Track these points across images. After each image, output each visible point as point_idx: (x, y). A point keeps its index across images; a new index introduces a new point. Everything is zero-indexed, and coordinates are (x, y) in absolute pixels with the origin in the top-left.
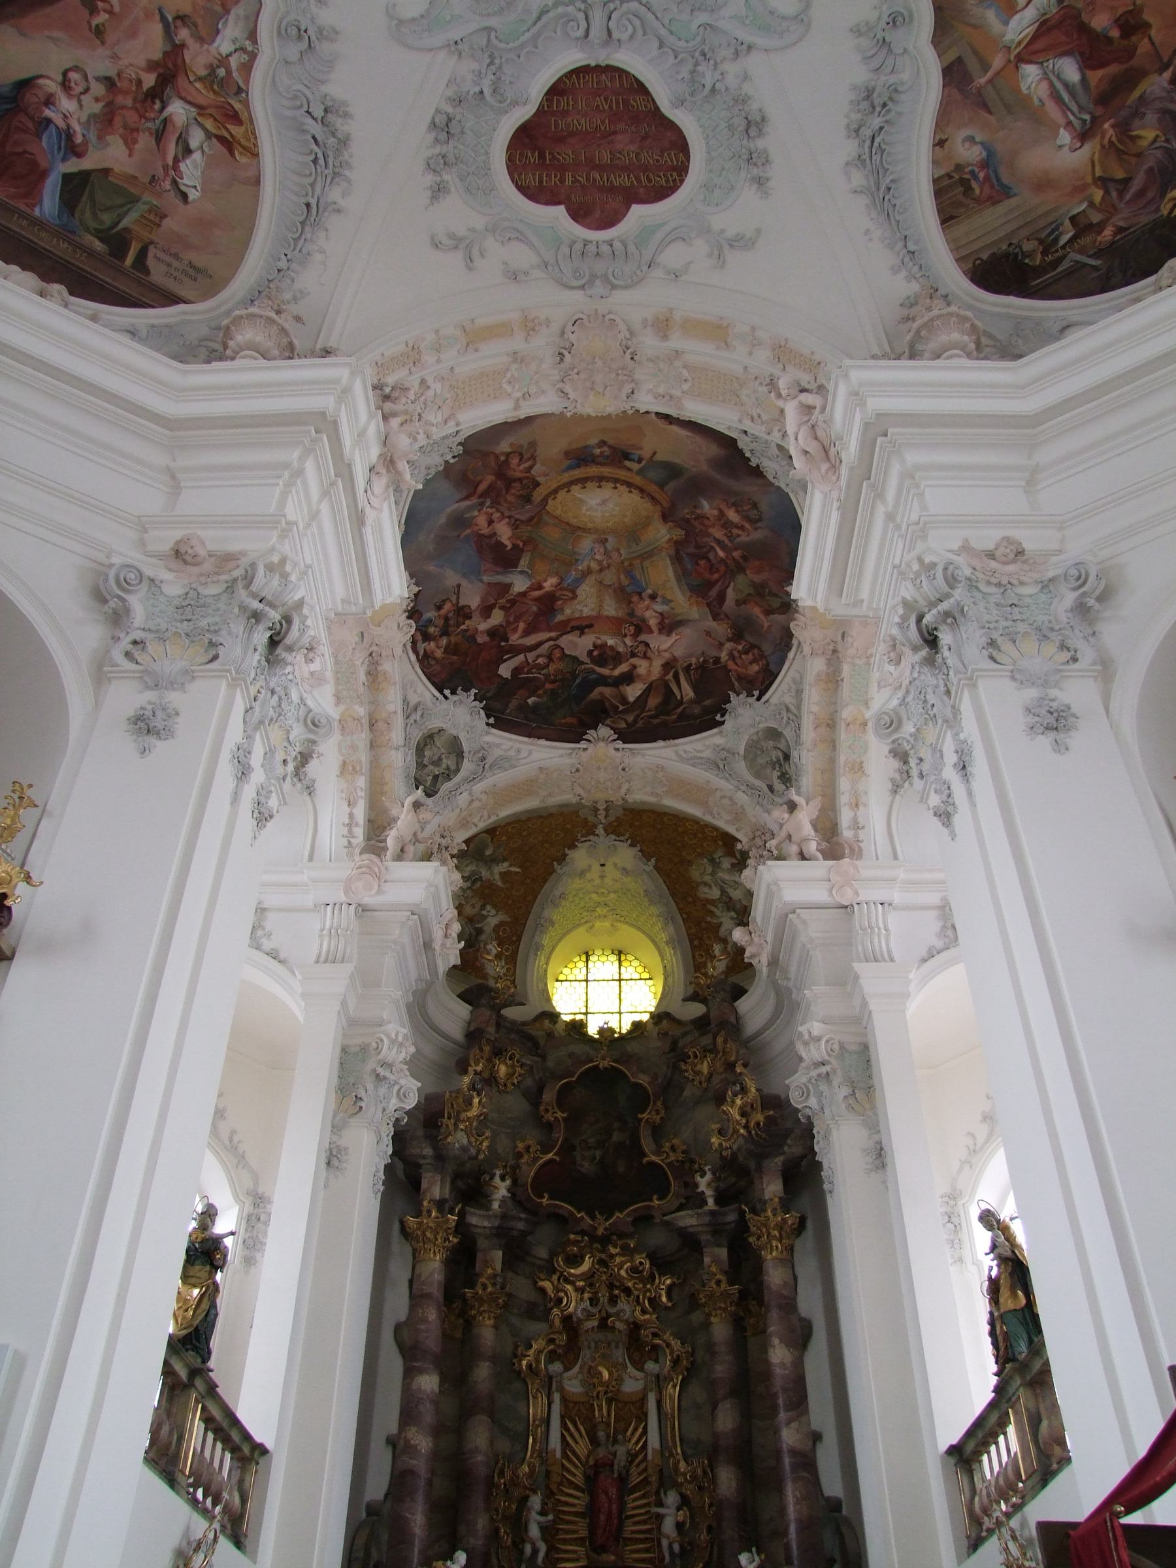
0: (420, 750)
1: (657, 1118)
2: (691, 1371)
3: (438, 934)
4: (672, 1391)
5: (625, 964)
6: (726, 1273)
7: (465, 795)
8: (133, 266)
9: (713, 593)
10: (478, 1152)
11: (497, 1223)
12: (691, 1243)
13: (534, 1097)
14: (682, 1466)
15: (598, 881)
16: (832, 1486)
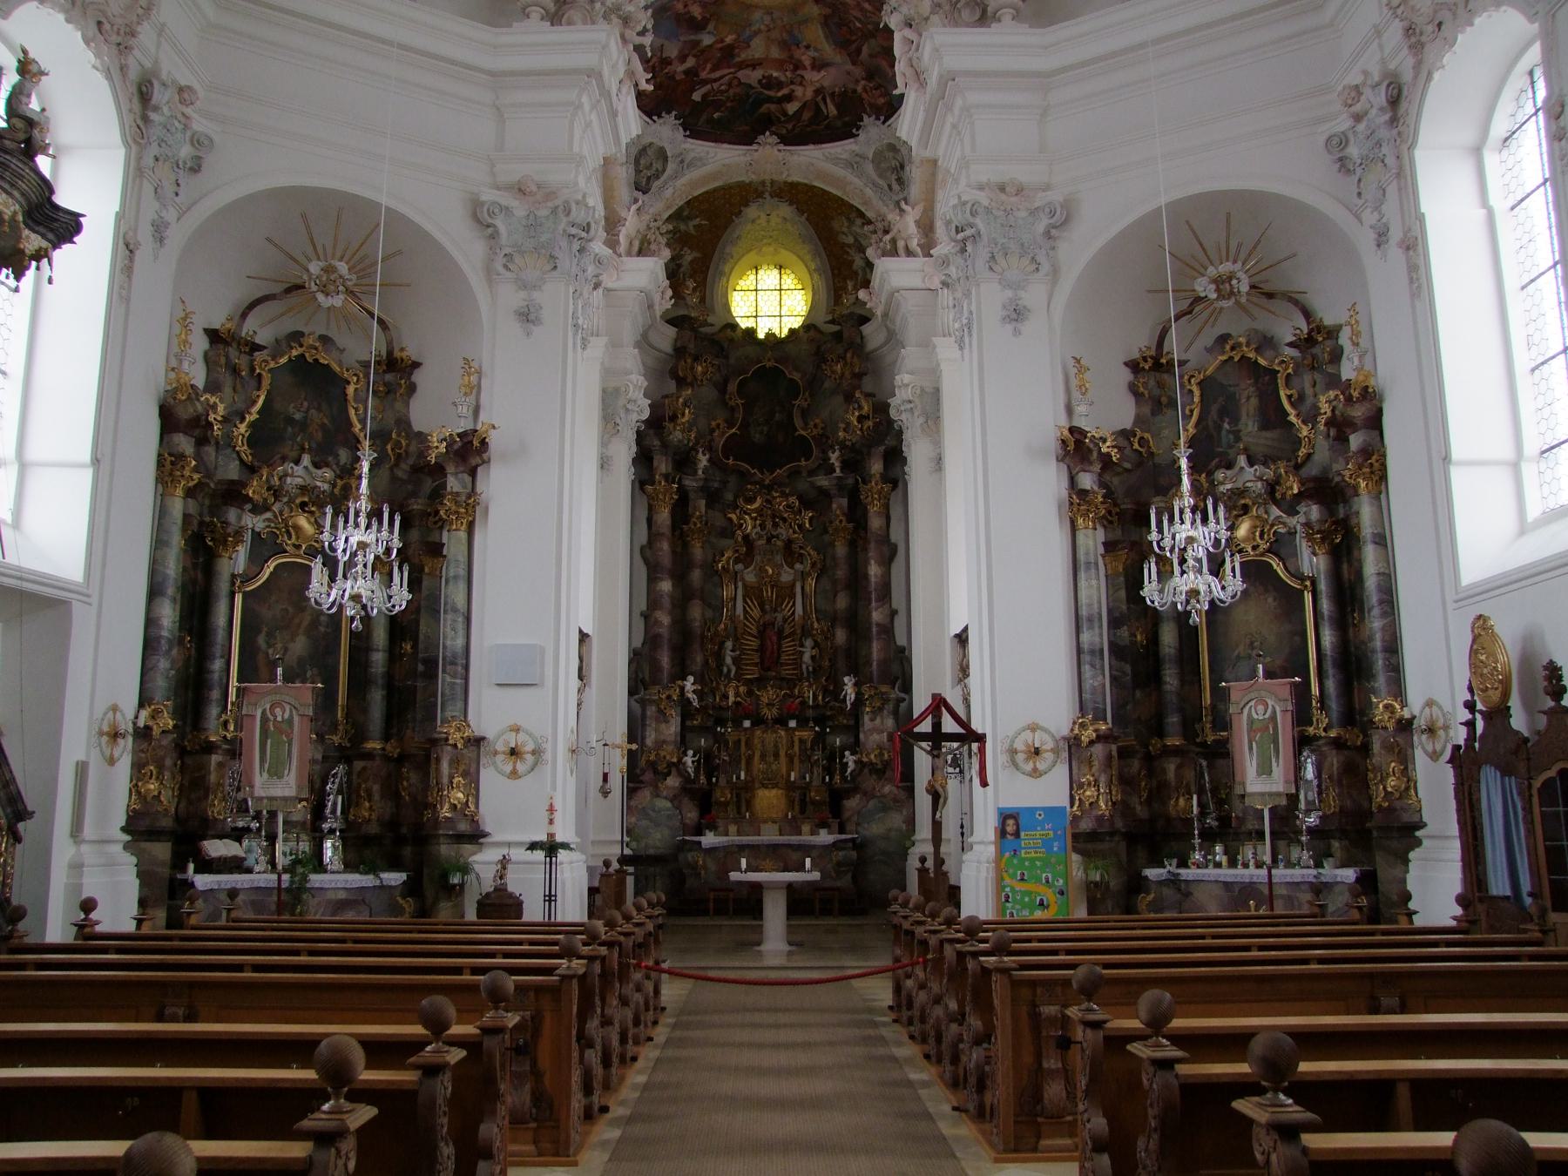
0: (637, 162)
1: (805, 404)
2: (823, 571)
3: (657, 298)
4: (811, 582)
5: (784, 277)
6: (844, 514)
7: (670, 190)
9: (854, 46)
10: (689, 440)
11: (701, 484)
12: (824, 494)
13: (722, 388)
14: (816, 625)
15: (764, 224)
16: (901, 640)
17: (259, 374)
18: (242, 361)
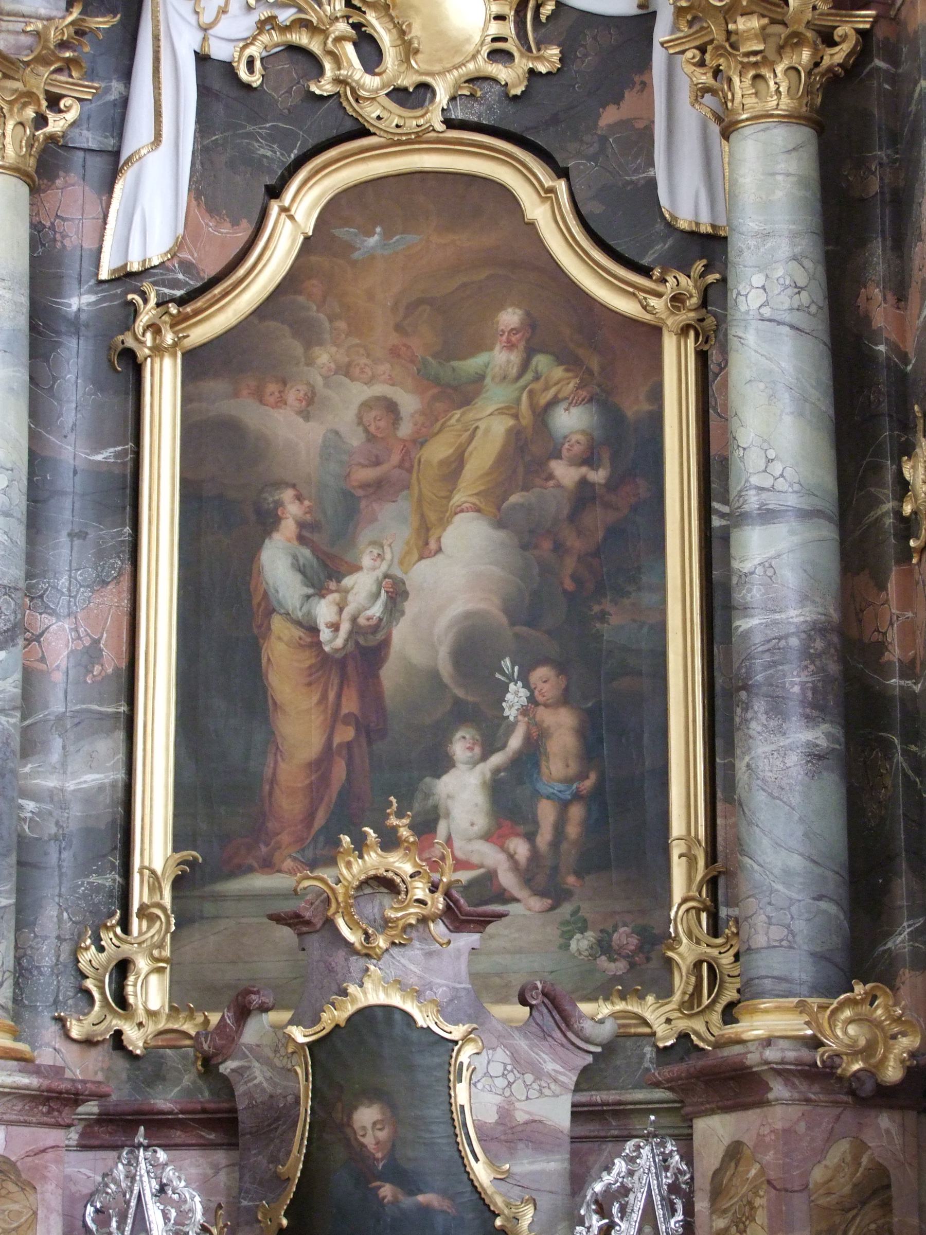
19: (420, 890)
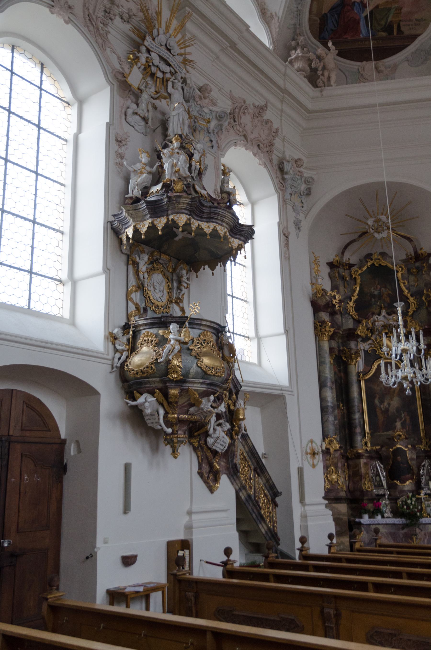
8: (397, 34)
17: (355, 278)
18: (346, 274)
19: (403, 436)
